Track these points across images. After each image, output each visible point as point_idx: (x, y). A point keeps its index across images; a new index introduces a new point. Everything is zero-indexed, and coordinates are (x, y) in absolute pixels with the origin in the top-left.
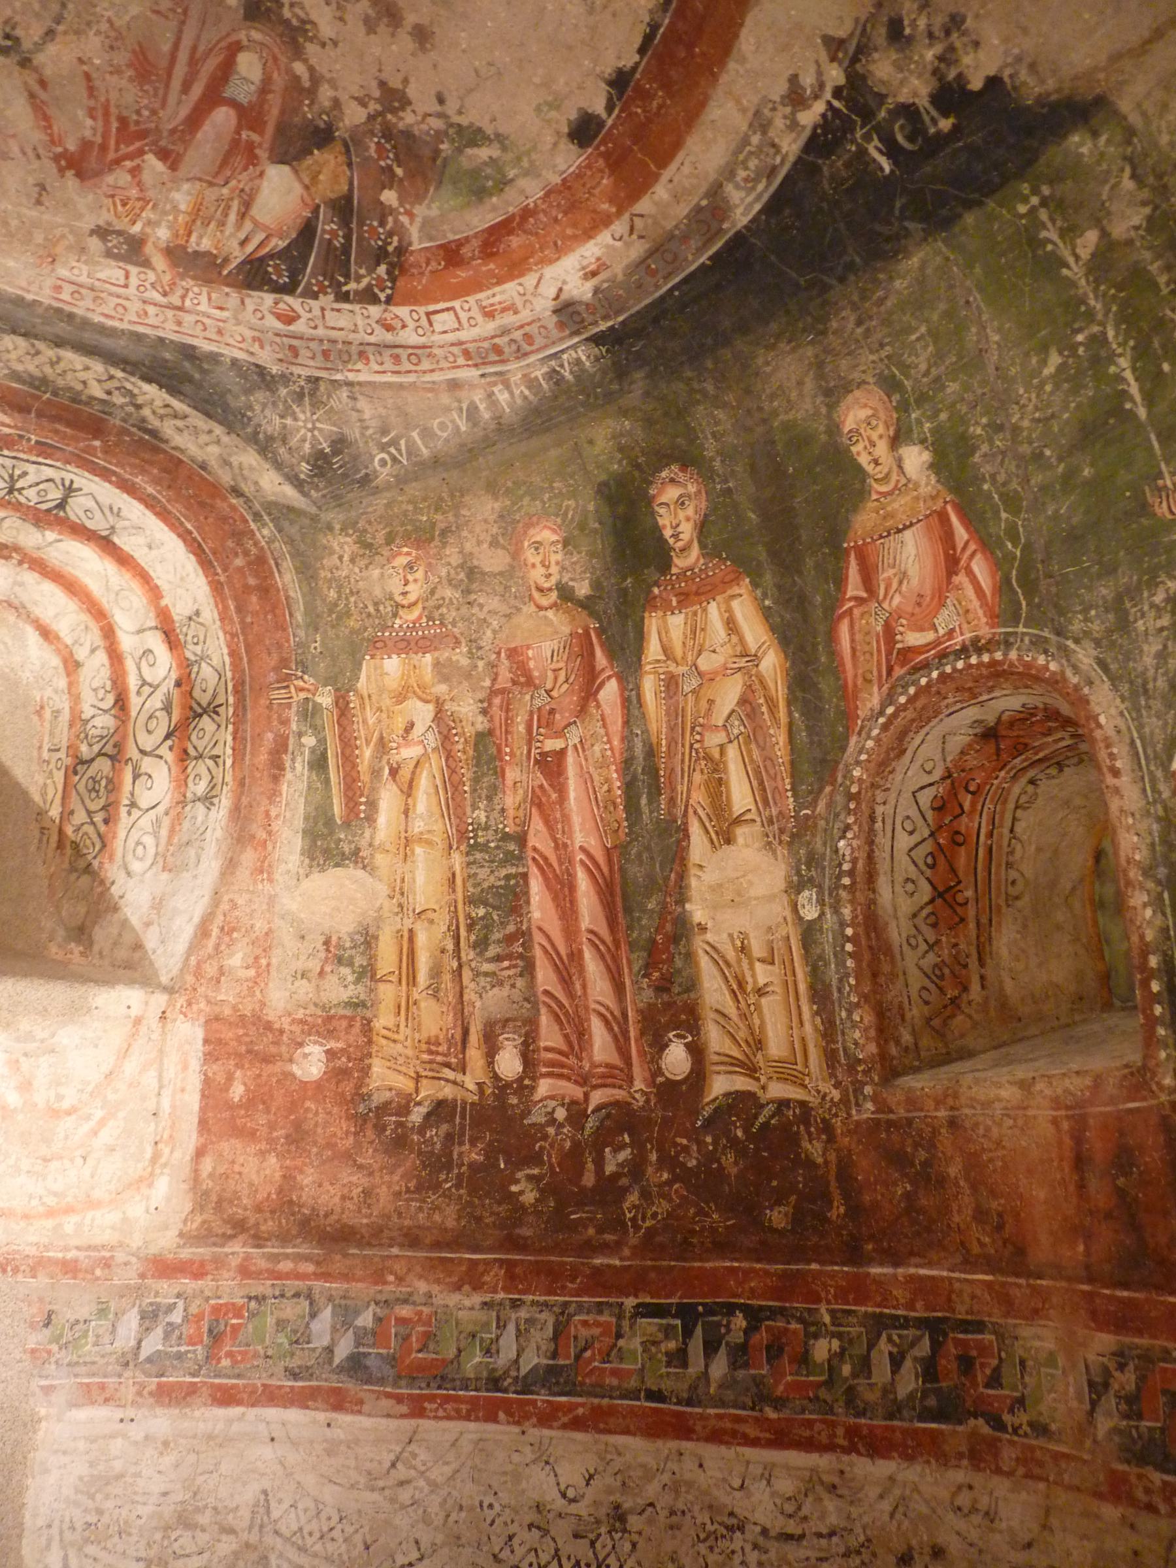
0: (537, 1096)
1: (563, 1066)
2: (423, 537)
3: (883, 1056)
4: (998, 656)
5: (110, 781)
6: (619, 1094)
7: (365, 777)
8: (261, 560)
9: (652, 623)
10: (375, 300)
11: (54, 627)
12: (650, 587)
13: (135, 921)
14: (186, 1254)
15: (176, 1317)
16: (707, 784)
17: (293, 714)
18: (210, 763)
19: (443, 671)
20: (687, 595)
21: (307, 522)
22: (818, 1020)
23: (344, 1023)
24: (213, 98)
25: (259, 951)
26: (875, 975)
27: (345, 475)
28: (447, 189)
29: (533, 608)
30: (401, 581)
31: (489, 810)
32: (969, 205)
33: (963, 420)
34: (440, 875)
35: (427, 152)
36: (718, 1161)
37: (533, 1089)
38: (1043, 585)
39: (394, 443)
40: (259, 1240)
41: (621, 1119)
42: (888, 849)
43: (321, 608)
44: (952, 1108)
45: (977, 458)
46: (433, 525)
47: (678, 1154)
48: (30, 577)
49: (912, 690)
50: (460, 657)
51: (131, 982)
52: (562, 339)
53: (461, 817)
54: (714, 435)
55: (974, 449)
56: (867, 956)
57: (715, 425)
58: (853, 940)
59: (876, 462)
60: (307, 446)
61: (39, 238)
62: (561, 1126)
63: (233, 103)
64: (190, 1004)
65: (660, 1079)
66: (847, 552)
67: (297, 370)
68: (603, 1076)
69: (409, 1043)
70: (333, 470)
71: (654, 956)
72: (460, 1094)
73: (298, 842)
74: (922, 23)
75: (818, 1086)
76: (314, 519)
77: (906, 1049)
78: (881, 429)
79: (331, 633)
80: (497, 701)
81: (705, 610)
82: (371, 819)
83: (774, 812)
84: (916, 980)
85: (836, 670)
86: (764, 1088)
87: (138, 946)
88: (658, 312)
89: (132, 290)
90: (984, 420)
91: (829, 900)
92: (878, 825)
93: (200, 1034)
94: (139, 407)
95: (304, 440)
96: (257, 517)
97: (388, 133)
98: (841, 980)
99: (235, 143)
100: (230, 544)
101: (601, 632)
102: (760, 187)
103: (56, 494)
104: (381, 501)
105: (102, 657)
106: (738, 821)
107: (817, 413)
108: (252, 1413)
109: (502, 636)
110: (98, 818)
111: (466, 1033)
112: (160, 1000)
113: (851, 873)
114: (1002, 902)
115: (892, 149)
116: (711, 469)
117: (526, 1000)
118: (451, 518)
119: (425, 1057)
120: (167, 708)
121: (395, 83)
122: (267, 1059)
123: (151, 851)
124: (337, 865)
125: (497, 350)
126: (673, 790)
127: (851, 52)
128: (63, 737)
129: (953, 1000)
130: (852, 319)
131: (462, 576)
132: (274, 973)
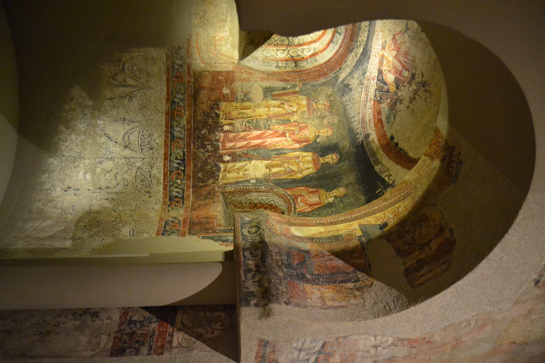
2: (331, 107)
3: (226, 192)
5: (283, 44)
6: (221, 148)
7: (281, 98)
8: (326, 74)
9: (310, 154)
10: (375, 97)
14: (191, 71)
15: (181, 70)
17: (294, 83)
19: (303, 113)
28: (389, 112)
30: (322, 103)
31: (275, 123)
39: (350, 101)
40: (194, 83)
41: (216, 149)
43: (316, 87)
50: (306, 116)
51: (240, 56)
58: (246, 188)
73: (268, 86)
75: (221, 182)
84: (240, 199)
85: (296, 187)
88: (365, 153)
93: (230, 70)
94: (357, 48)
96: (335, 73)
97: (397, 100)
100: (329, 68)
101: (310, 144)
104: (339, 99)
105: (310, 40)
106: (270, 169)
108: (165, 85)
110: (276, 43)
111: (232, 120)
112: (236, 62)
115: (379, 193)
120: (298, 56)
122: (226, 83)
123: (267, 55)
125: (364, 122)
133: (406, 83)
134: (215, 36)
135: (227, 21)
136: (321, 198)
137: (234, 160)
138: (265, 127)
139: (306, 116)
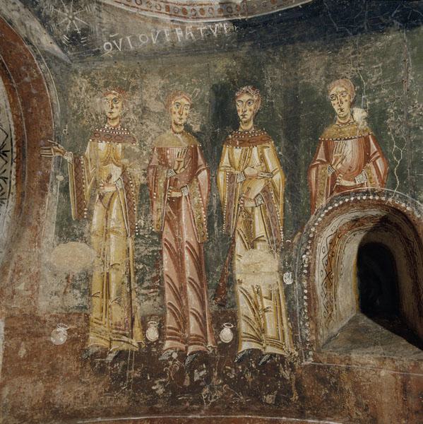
1: (176, 335)
2: (123, 88)
4: (383, 198)
6: (201, 348)
7: (87, 199)
9: (226, 150)
16: (245, 222)
20: (244, 141)
21: (64, 66)
22: (290, 324)
23: (76, 317)
25: (33, 282)
27: (87, 48)
29: (171, 132)
30: (110, 106)
31: (145, 221)
36: (244, 376)
38: (409, 177)
39: (116, 39)
44: (348, 364)
47: (226, 373)
49: (341, 202)
50: (135, 147)
52: (218, 17)
53: (132, 222)
54: (271, 79)
57: (274, 75)
59: (342, 110)
60: (68, 27)
62: (175, 360)
65: (219, 342)
66: (320, 142)
68: (194, 340)
69: (107, 325)
71: (218, 291)
72: (130, 348)
73: (53, 228)
75: (288, 349)
76: (68, 66)
78: (347, 98)
80: (151, 171)
81: (251, 150)
82: (89, 219)
86: (264, 348)
90: (395, 108)
96: (38, 57)
98: (301, 310)
101: (201, 149)
106: (257, 240)
107: (320, 84)
111: (133, 320)
116: (266, 93)
117: (160, 306)
119: (114, 331)
124: (73, 240)
125: (185, 11)
126: (229, 222)
130: (351, 51)
132: (41, 293)
137: (233, 319)
138: (154, 243)
139: (135, 147)
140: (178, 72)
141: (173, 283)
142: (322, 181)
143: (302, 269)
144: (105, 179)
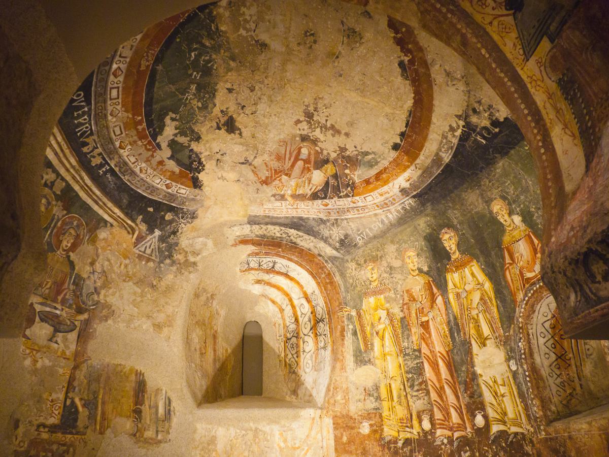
0: (437, 435)
1: (443, 425)
2: (375, 259)
3: (545, 416)
5: (297, 344)
6: (463, 433)
7: (369, 336)
8: (329, 274)
9: (449, 276)
10: (349, 196)
11: (276, 300)
12: (446, 266)
13: (309, 387)
16: (475, 327)
17: (345, 319)
18: (324, 337)
19: (387, 300)
22: (522, 404)
23: (374, 415)
24: (297, 159)
25: (345, 394)
26: (538, 388)
27: (349, 245)
28: (362, 166)
30: (370, 274)
31: (408, 342)
32: (511, 148)
33: (528, 207)
34: (396, 365)
35: (355, 159)
36: (498, 454)
37: (435, 433)
41: (465, 442)
42: (536, 344)
43: (348, 285)
44: (569, 433)
45: (535, 218)
46: (377, 255)
48: (267, 287)
49: (532, 292)
51: (310, 407)
54: (455, 218)
55: (533, 216)
56: (534, 381)
57: (455, 215)
59: (506, 221)
61: (258, 200)
62: (446, 445)
63: (302, 159)
64: (327, 412)
65: (475, 428)
66: (503, 249)
67: (331, 218)
68: (457, 427)
69: (394, 420)
70: (346, 244)
74: (481, 108)
75: (526, 428)
76: (342, 259)
77: (554, 412)
78: (505, 211)
79: (352, 293)
81: (464, 271)
82: (372, 349)
83: (497, 335)
84: (554, 389)
85: (508, 286)
86: (509, 429)
87: (311, 395)
88: (429, 188)
89: (284, 207)
91: (519, 362)
92: (531, 336)
93: (332, 422)
94: (290, 237)
95: (336, 237)
96: (326, 261)
97: (343, 157)
98: (527, 390)
99: (304, 168)
100: (320, 271)
101: (433, 281)
102: (450, 152)
103: (271, 265)
104: (361, 251)
105: (290, 307)
106: (486, 339)
107: (484, 209)
109: (403, 286)
110: (295, 356)
112: (319, 412)
113: (524, 354)
114: (585, 357)
115: (484, 138)
116: (457, 228)
118: (382, 252)
120: (310, 321)
121: (343, 146)
122: (352, 428)
123: (311, 365)
124: (364, 365)
125: (386, 204)
126: (464, 330)
127: (465, 117)
128: (282, 332)
129: (570, 394)
130: (487, 181)
131: (388, 269)
133: (317, 148)
134: (280, 448)
135: (256, 429)
136: (518, 237)
137: (481, 407)
138: (417, 357)
140: (401, 238)
141: (434, 384)
142: (515, 279)
143: (521, 356)
144: (378, 320)
